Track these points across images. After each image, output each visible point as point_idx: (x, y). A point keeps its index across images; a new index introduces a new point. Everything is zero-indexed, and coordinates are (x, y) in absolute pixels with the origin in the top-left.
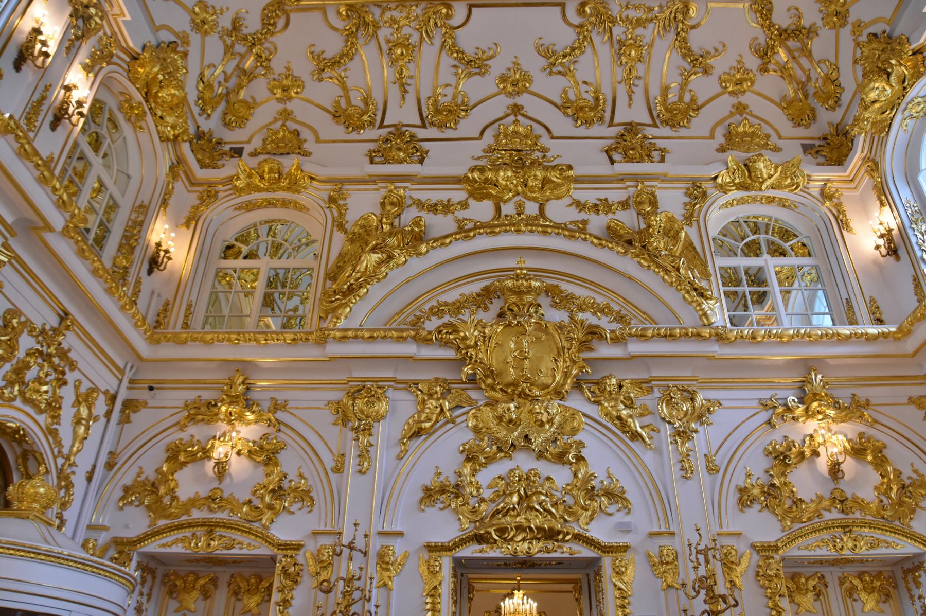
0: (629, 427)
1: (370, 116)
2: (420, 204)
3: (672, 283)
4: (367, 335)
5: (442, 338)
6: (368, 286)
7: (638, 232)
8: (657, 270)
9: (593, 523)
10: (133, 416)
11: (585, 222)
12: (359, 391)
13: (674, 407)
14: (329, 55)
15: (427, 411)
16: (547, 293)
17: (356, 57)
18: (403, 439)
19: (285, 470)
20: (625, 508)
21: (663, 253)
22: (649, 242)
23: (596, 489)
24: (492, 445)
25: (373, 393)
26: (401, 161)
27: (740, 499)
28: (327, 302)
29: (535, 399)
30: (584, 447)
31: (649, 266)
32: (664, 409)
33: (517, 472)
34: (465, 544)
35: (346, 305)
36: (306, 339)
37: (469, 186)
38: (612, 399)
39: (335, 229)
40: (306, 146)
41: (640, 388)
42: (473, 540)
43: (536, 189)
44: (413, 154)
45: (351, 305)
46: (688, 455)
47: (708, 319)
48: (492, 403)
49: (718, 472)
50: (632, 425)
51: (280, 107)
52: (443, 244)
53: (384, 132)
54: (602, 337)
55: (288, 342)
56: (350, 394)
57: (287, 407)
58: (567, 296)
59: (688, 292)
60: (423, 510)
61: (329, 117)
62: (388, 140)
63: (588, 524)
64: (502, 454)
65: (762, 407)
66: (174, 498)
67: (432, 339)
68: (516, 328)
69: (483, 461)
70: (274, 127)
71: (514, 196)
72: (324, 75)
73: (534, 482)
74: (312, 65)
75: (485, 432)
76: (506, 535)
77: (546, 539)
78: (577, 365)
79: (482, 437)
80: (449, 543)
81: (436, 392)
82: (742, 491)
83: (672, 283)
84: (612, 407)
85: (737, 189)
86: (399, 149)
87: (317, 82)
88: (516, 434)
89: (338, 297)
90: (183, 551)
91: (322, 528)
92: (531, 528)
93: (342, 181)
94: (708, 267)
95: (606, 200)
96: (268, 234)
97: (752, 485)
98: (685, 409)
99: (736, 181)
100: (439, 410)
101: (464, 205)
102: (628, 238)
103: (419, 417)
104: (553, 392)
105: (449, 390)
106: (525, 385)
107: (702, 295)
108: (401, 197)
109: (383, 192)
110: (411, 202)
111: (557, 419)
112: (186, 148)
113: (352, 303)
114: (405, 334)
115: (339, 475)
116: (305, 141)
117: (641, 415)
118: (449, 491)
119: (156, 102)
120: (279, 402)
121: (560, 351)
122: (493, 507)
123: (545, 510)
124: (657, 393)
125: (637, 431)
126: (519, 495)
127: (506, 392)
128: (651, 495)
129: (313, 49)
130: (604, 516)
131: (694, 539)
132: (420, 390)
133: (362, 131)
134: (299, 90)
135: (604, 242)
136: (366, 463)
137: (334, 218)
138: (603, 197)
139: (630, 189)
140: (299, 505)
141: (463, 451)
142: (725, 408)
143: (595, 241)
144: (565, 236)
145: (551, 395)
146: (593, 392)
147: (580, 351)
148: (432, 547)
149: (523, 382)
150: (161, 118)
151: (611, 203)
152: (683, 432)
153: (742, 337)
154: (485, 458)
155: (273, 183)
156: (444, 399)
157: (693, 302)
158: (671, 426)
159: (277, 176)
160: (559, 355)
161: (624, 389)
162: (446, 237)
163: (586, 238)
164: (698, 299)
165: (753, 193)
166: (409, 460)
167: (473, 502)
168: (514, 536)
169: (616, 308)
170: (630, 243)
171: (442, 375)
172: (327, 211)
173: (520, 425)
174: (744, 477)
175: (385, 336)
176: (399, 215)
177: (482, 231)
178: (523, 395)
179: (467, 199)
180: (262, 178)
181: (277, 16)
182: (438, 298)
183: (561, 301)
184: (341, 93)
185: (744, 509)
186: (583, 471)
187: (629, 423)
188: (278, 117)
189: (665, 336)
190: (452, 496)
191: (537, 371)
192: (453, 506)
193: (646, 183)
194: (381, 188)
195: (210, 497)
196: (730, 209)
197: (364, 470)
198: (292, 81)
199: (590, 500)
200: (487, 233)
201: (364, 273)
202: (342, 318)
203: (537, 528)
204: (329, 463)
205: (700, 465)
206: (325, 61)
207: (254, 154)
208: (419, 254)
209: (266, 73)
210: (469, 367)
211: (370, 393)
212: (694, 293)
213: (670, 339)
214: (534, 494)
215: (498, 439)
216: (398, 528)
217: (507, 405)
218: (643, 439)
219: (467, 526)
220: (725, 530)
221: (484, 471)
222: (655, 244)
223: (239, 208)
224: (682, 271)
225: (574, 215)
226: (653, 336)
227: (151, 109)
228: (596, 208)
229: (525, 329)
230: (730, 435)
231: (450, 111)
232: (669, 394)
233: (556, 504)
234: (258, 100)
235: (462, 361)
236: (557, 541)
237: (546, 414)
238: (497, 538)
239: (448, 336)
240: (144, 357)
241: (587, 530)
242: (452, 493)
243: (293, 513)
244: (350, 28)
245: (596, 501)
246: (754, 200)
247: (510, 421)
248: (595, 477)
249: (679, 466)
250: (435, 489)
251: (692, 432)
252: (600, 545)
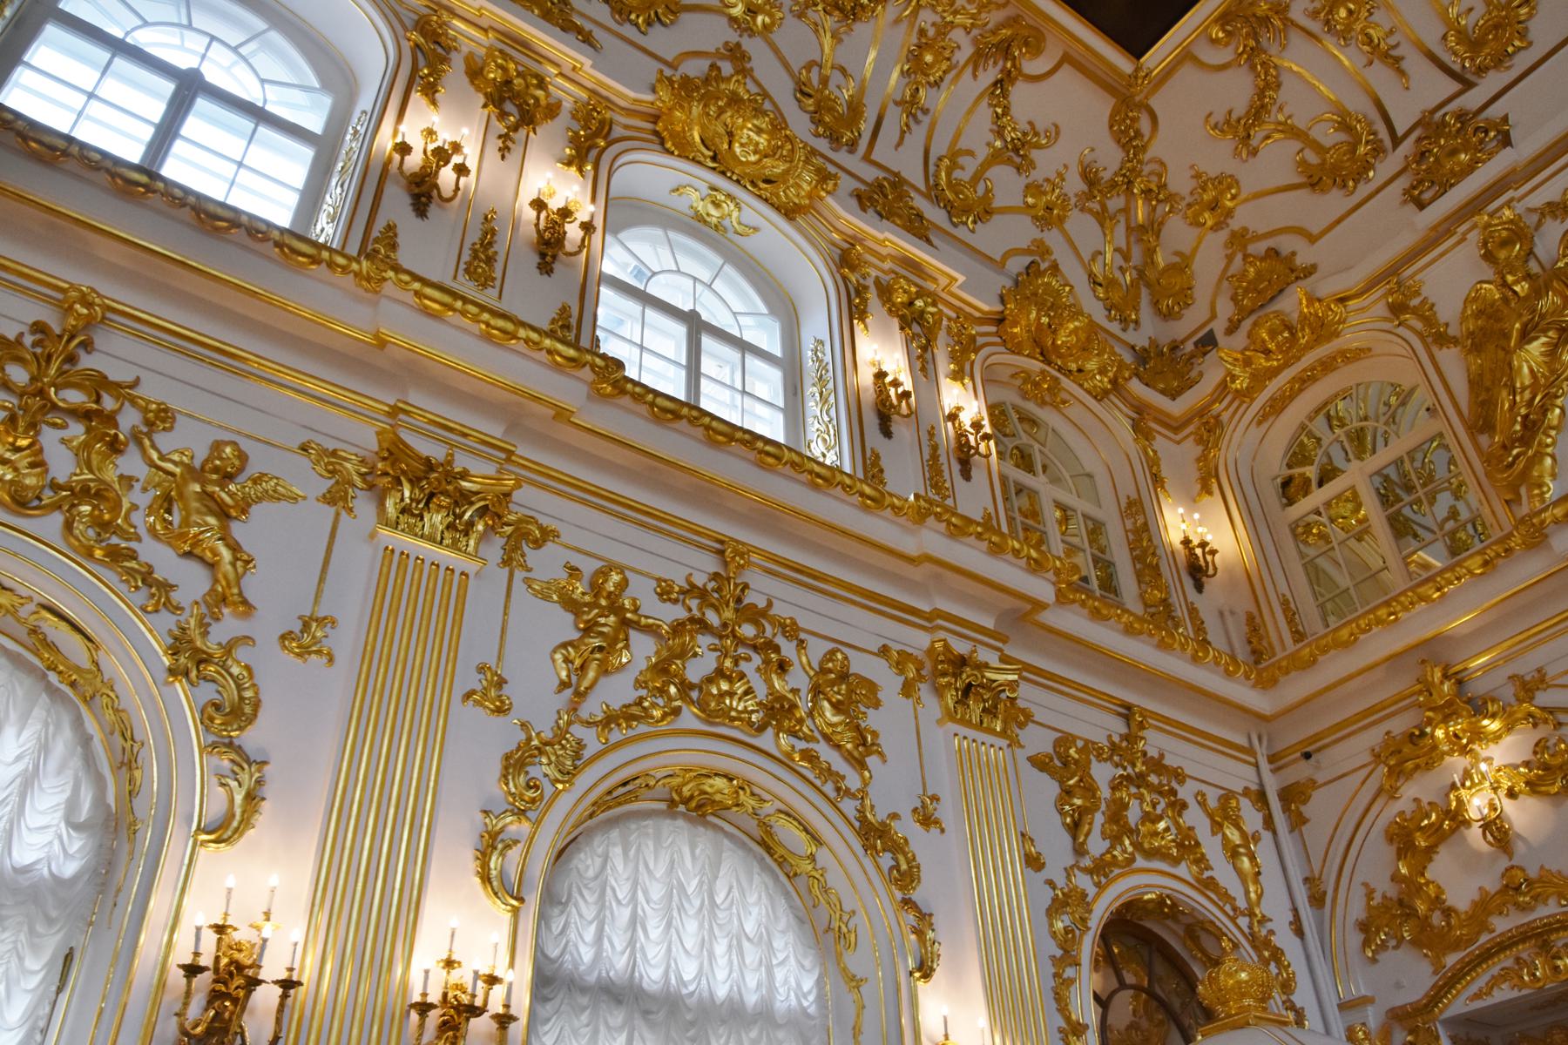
1: (1367, 142)
6: (1559, 402)
10: (1307, 810)
14: (1240, 107)
17: (1284, 78)
26: (1470, 168)
28: (1503, 472)
35: (1540, 456)
36: (1506, 551)
39: (1435, 349)
40: (1300, 261)
44: (1481, 141)
45: (1549, 450)
51: (1223, 235)
53: (1407, 147)
55: (1478, 571)
57: (1547, 678)
61: (1303, 194)
62: (1423, 154)
66: (1448, 912)
70: (1233, 269)
72: (1254, 142)
74: (1227, 144)
86: (1454, 152)
87: (1251, 160)
89: (1515, 452)
90: (1515, 994)
93: (1392, 271)
96: (1331, 427)
108: (1511, 221)
109: (1474, 237)
110: (1535, 218)
112: (1136, 387)
113: (1548, 446)
116: (1294, 254)
119: (1060, 356)
120: (1528, 678)
129: (1212, 121)
133: (1371, 174)
134: (1233, 191)
137: (1419, 334)
150: (1080, 371)
155: (1289, 348)
159: (1286, 335)
172: (1401, 330)
176: (1531, 253)
180: (1267, 352)
181: (1133, 120)
184: (1297, 145)
188: (1230, 251)
194: (1464, 234)
195: (1507, 886)
198: (1215, 188)
201: (1535, 387)
202: (1548, 480)
206: (1242, 122)
207: (1232, 329)
209: (1172, 207)
223: (1263, 417)
227: (1060, 369)
231: (1496, 27)
234: (1186, 250)
240: (1268, 713)
244: (1245, 46)
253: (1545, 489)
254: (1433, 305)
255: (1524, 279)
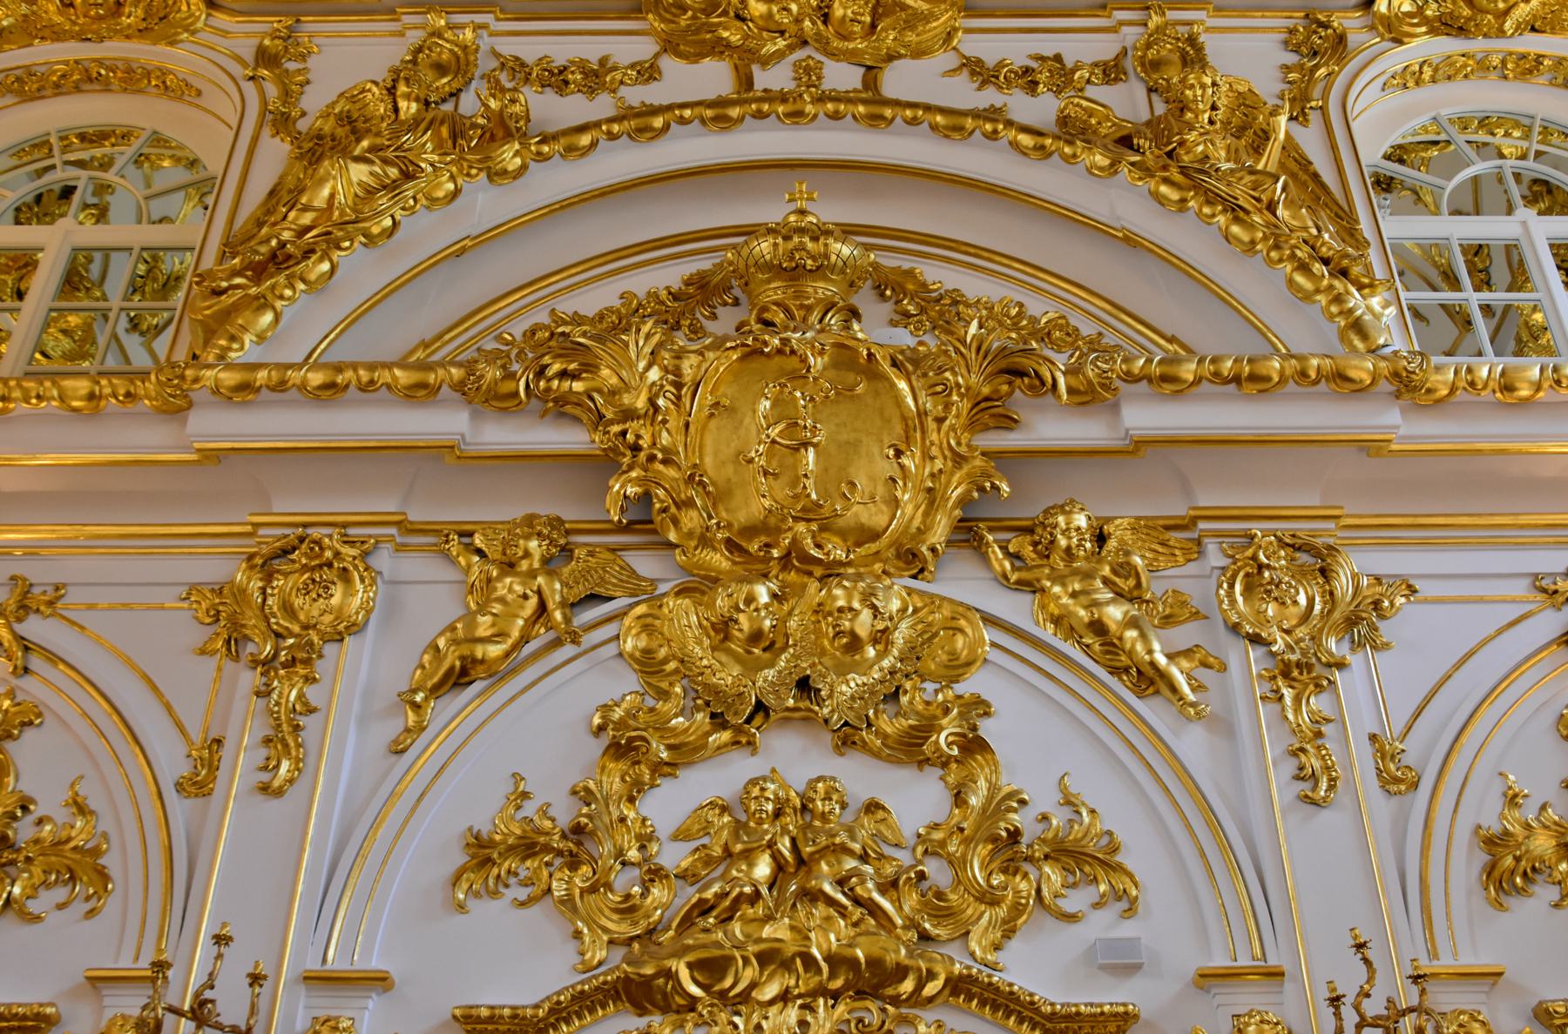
0: (1131, 653)
2: (519, 69)
3: (1253, 242)
4: (316, 378)
5: (548, 390)
6: (336, 255)
7: (1148, 123)
8: (1207, 210)
9: (1014, 944)
11: (991, 114)
12: (285, 552)
13: (1269, 592)
15: (497, 608)
16: (879, 290)
18: (414, 691)
19: (27, 787)
20: (1119, 899)
21: (1225, 166)
22: (1182, 143)
23: (1024, 840)
24: (698, 709)
25: (328, 554)
27: (1490, 870)
29: (831, 572)
30: (987, 714)
31: (1183, 201)
32: (1240, 599)
33: (772, 787)
34: (592, 1011)
35: (262, 304)
36: (128, 395)
37: (663, 20)
38: (1076, 573)
39: (267, 131)
41: (1162, 544)
42: (617, 997)
43: (857, 28)
45: (279, 304)
46: (1319, 734)
47: (1364, 336)
48: (698, 586)
49: (1415, 785)
50: (1139, 647)
52: (570, 149)
54: (1042, 387)
55: (76, 404)
56: (259, 561)
57: (59, 605)
58: (938, 301)
59: (1303, 268)
60: (461, 907)
63: (997, 948)
64: (726, 736)
65: (1541, 597)
67: (517, 393)
68: (777, 359)
69: (664, 755)
71: (791, 48)
73: (824, 817)
75: (676, 671)
76: (728, 983)
77: (860, 994)
78: (966, 468)
79: (664, 685)
80: (537, 1006)
81: (527, 554)
82: (1494, 843)
83: (1253, 242)
84: (1074, 595)
85: (1433, 31)
88: (770, 673)
89: (238, 281)
91: (126, 961)
92: (809, 961)
94: (1357, 221)
95: (1058, 58)
97: (1528, 827)
98: (1302, 599)
99: (1429, 13)
100: (533, 601)
101: (648, 72)
102: (1119, 135)
103: (470, 622)
104: (891, 553)
105: (567, 552)
106: (801, 527)
107: (1344, 273)
108: (465, 48)
109: (415, 37)
111: (900, 637)
114: (431, 378)
115: (200, 800)
117: (1168, 621)
118: (547, 849)
121: (913, 426)
122: (691, 895)
123: (857, 901)
124: (1215, 556)
125: (1153, 664)
126: (776, 857)
127: (743, 551)
128: (1203, 854)
130: (1050, 922)
131: (1350, 980)
132: (479, 552)
135: (1048, 142)
136: (285, 766)
138: (1049, 53)
139: (1125, 29)
140: (61, 894)
141: (601, 728)
142: (1426, 601)
143: (1026, 140)
144: (934, 127)
145: (885, 561)
146: (1016, 556)
147: (974, 425)
148: (479, 1020)
149: (796, 519)
151: (1069, 64)
152: (1298, 665)
153: (1472, 384)
154: (670, 747)
155: (100, 18)
156: (552, 575)
157: (1318, 291)
158: (1261, 650)
160: (908, 439)
161: (1112, 544)
162: (582, 129)
163: (995, 131)
164: (1336, 283)
165: (1477, 45)
166: (428, 753)
167: (625, 881)
168: (753, 985)
169: (1087, 328)
170: (1126, 142)
171: (545, 509)
172: (250, 88)
173: (786, 647)
174: (1495, 803)
175: (372, 382)
177: (687, 113)
178: (795, 558)
179: (657, 56)
182: (551, 304)
183: (923, 311)
185: (1503, 899)
186: (982, 784)
187: (1128, 646)
189: (1237, 379)
190: (558, 862)
191: (839, 480)
192: (559, 890)
193: (1172, 15)
196: (1416, 95)
197: (276, 784)
199: (1005, 871)
200: (703, 121)
202: (248, 339)
203: (829, 958)
204: (172, 761)
205: (1362, 761)
208: (497, 175)
210: (634, 474)
211: (320, 556)
212: (1318, 267)
213: (1251, 388)
214: (822, 852)
215: (716, 691)
216: (375, 963)
217: (746, 588)
218: (1174, 689)
219: (600, 954)
220: (1445, 963)
221: (666, 787)
222: (1200, 148)
224: (1281, 211)
225: (965, 94)
226: (1198, 381)
228: (1028, 80)
229: (804, 360)
230: (1447, 677)
232: (1254, 558)
233: (894, 884)
235: (606, 464)
236: (896, 1001)
237: (866, 615)
238: (695, 990)
239: (566, 384)
241: (994, 967)
242: (560, 853)
243: (37, 918)
245: (1025, 875)
246: (1483, 66)
247: (756, 636)
248: (1023, 802)
249: (1290, 766)
250: (504, 842)
251: (1329, 665)
252: (1037, 1011)
253: (235, 346)
254: (308, 82)
255: (417, 100)
